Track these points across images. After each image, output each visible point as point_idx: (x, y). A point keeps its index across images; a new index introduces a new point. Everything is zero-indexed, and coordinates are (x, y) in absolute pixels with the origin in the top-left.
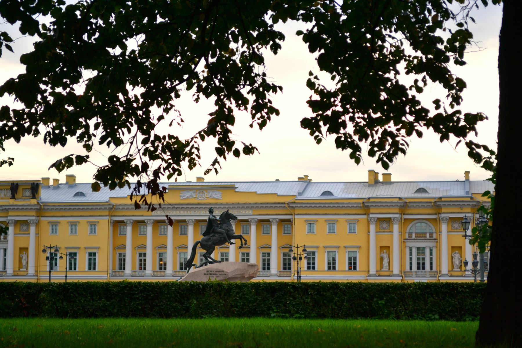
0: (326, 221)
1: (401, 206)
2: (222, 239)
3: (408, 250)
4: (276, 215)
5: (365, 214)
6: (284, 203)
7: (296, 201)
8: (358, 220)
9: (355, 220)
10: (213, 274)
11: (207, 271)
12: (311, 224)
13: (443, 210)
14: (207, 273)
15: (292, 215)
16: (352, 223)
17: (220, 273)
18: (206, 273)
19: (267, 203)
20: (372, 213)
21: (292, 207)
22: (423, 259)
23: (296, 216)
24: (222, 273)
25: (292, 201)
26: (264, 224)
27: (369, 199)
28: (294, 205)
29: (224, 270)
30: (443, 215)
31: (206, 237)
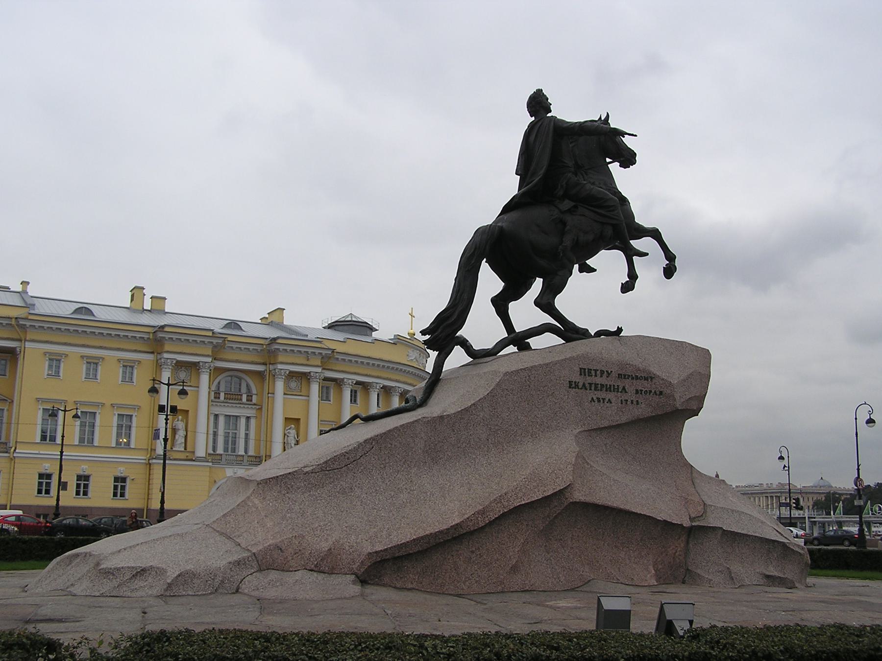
0: (82, 357)
1: (215, 347)
2: (609, 231)
3: (212, 418)
5: (152, 353)
7: (31, 317)
8: (139, 362)
9: (134, 361)
10: (609, 389)
11: (582, 371)
12: (55, 361)
13: (281, 358)
14: (580, 380)
15: (20, 340)
16: (128, 367)
18: (577, 378)
20: (168, 352)
21: (23, 327)
22: (235, 437)
23: (27, 343)
25: (23, 316)
27: (163, 327)
28: (28, 324)
29: (655, 370)
30: (280, 366)
31: (541, 214)
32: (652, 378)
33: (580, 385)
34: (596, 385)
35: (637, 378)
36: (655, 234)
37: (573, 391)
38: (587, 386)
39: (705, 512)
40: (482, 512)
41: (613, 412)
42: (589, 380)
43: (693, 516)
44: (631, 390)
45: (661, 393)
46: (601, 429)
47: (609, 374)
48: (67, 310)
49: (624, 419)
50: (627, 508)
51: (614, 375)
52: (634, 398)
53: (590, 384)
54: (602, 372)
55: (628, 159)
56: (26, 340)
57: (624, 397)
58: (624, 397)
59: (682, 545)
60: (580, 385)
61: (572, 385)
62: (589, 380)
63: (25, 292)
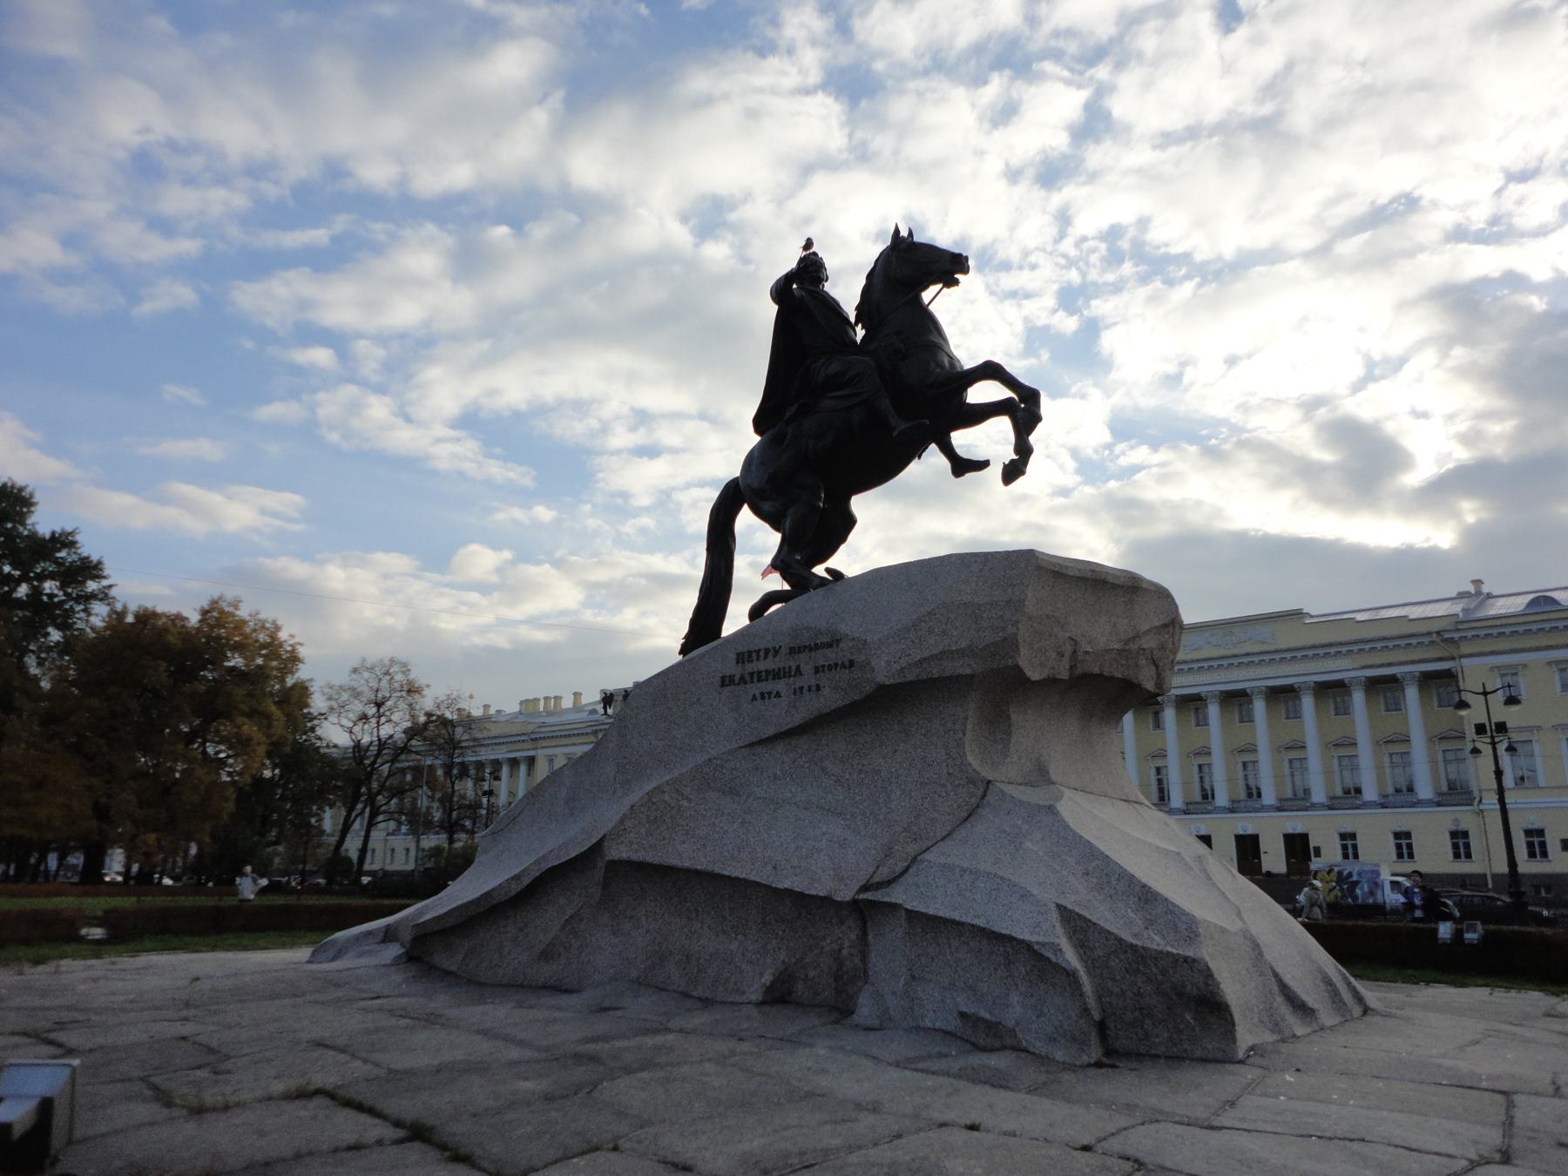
0: (1549, 664)
4: (1413, 662)
6: (1429, 634)
10: (776, 675)
15: (1453, 659)
17: (821, 658)
19: (1385, 639)
21: (1451, 641)
23: (1464, 661)
24: (831, 655)
26: (1383, 687)
31: (767, 435)
32: (838, 641)
33: (737, 679)
34: (759, 672)
35: (817, 647)
36: (991, 371)
37: (726, 691)
38: (747, 678)
39: (906, 870)
40: (517, 878)
41: (783, 713)
42: (750, 667)
43: (876, 879)
44: (807, 669)
45: (852, 663)
46: (761, 742)
47: (776, 652)
48: (1518, 604)
49: (798, 719)
50: (717, 870)
51: (784, 651)
52: (813, 683)
53: (751, 674)
54: (767, 651)
55: (947, 266)
56: (1461, 657)
57: (799, 682)
58: (799, 682)
59: (853, 937)
60: (737, 679)
61: (726, 681)
62: (750, 667)
63: (1479, 593)
